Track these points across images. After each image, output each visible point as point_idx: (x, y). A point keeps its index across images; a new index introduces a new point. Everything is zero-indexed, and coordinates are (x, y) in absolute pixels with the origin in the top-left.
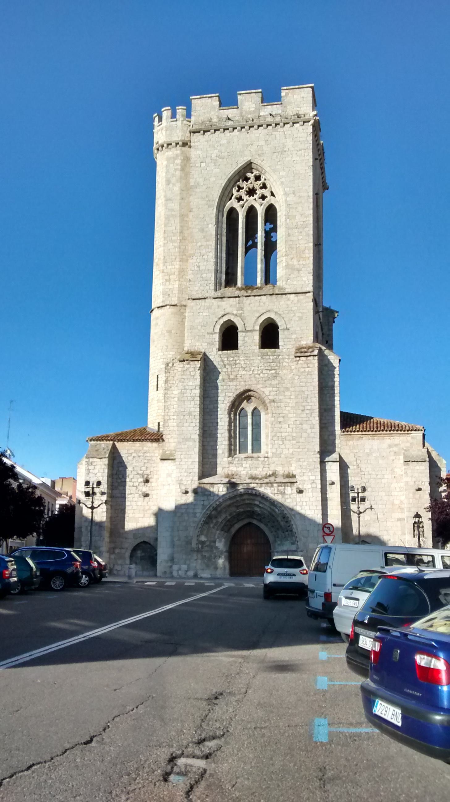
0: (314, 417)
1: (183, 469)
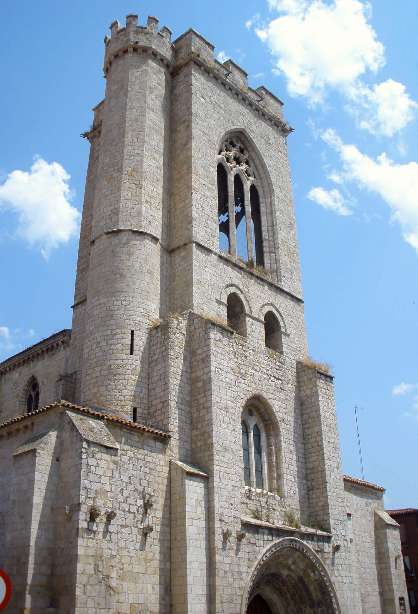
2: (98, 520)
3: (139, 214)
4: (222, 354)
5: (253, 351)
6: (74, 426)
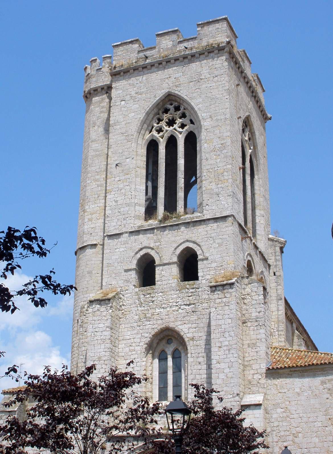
0: (233, 354)
5: (162, 293)
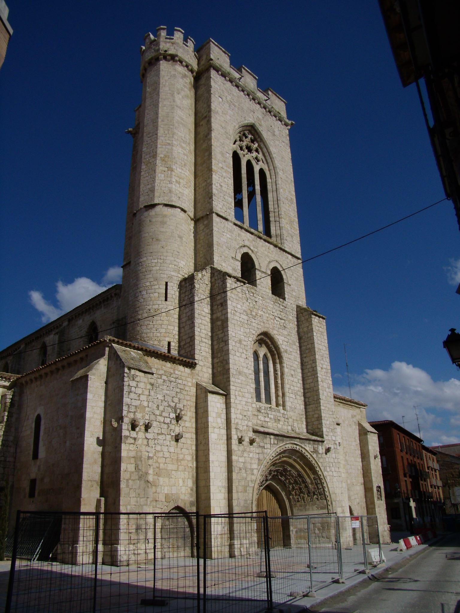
1: (238, 409)
2: (137, 429)
3: (170, 191)
4: (236, 299)
6: (118, 356)
